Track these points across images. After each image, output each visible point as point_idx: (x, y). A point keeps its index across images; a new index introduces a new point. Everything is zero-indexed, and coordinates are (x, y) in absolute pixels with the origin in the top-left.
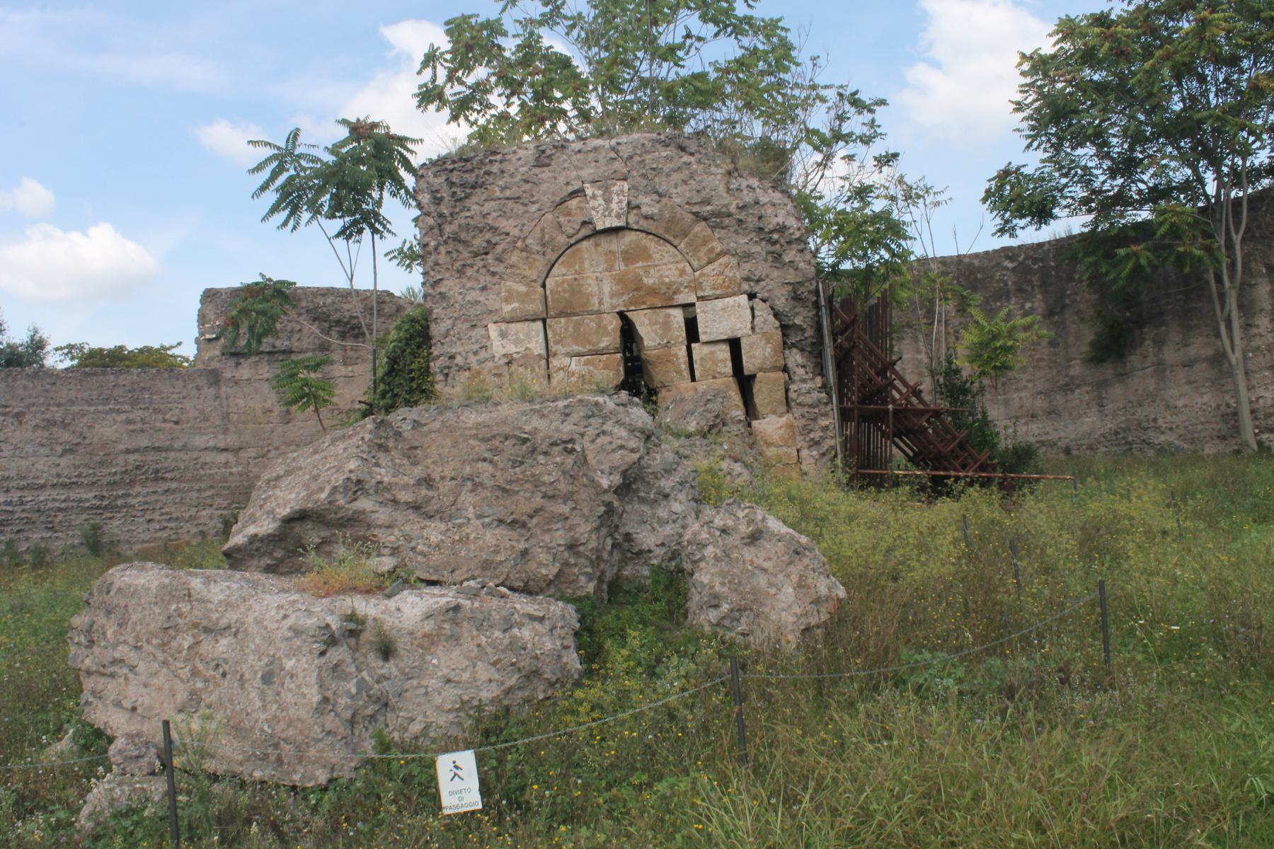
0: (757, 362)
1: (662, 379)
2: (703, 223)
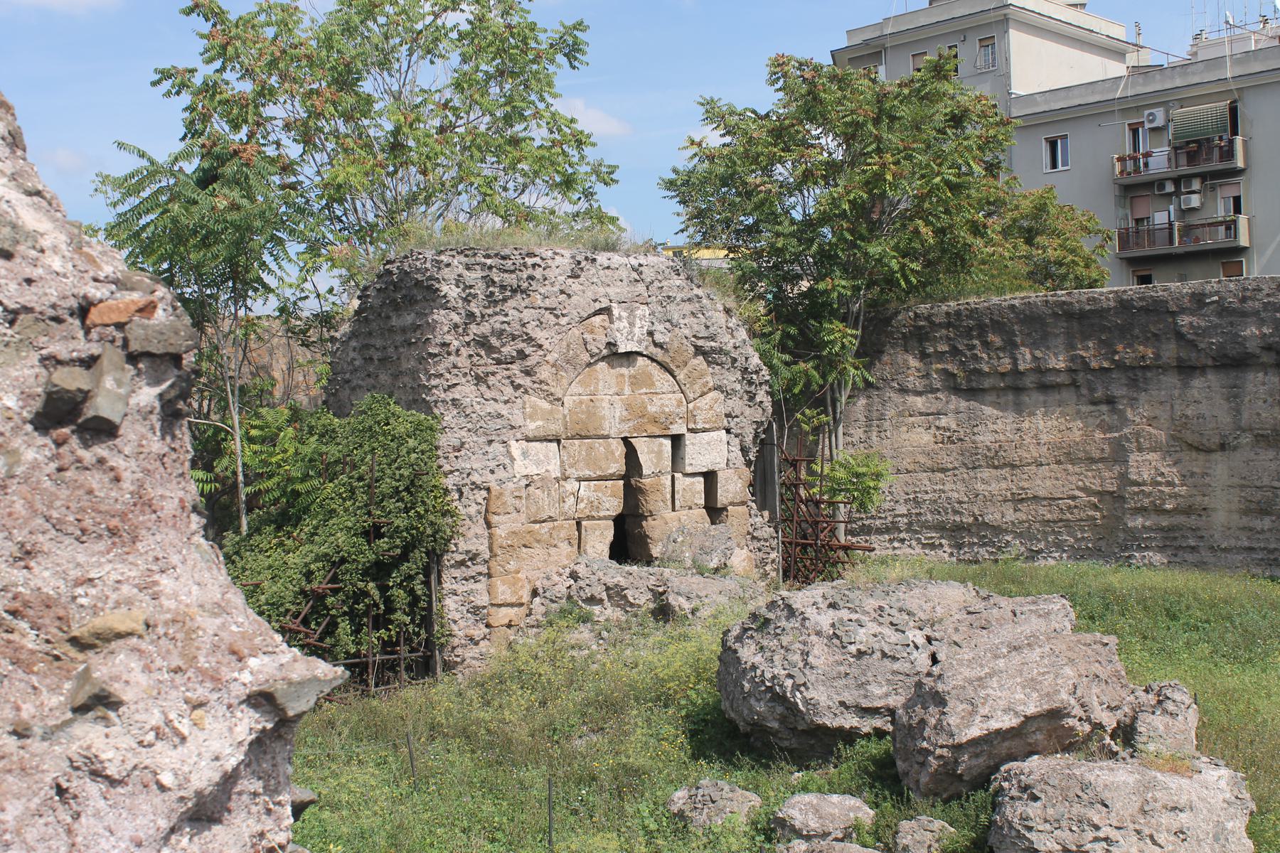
0: (730, 497)
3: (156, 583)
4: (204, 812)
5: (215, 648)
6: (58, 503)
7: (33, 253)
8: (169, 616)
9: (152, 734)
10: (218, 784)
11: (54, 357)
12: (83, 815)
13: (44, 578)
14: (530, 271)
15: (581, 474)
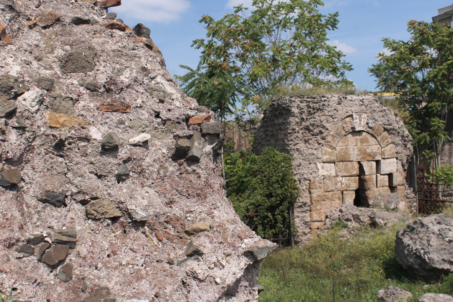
0: (398, 182)
1: (369, 187)
2: (386, 132)
3: (213, 213)
4: (230, 292)
5: (233, 235)
6: (180, 185)
7: (170, 101)
8: (217, 224)
9: (213, 264)
10: (234, 283)
11: (178, 136)
12: (191, 292)
13: (176, 211)
14: (323, 103)
15: (343, 175)
